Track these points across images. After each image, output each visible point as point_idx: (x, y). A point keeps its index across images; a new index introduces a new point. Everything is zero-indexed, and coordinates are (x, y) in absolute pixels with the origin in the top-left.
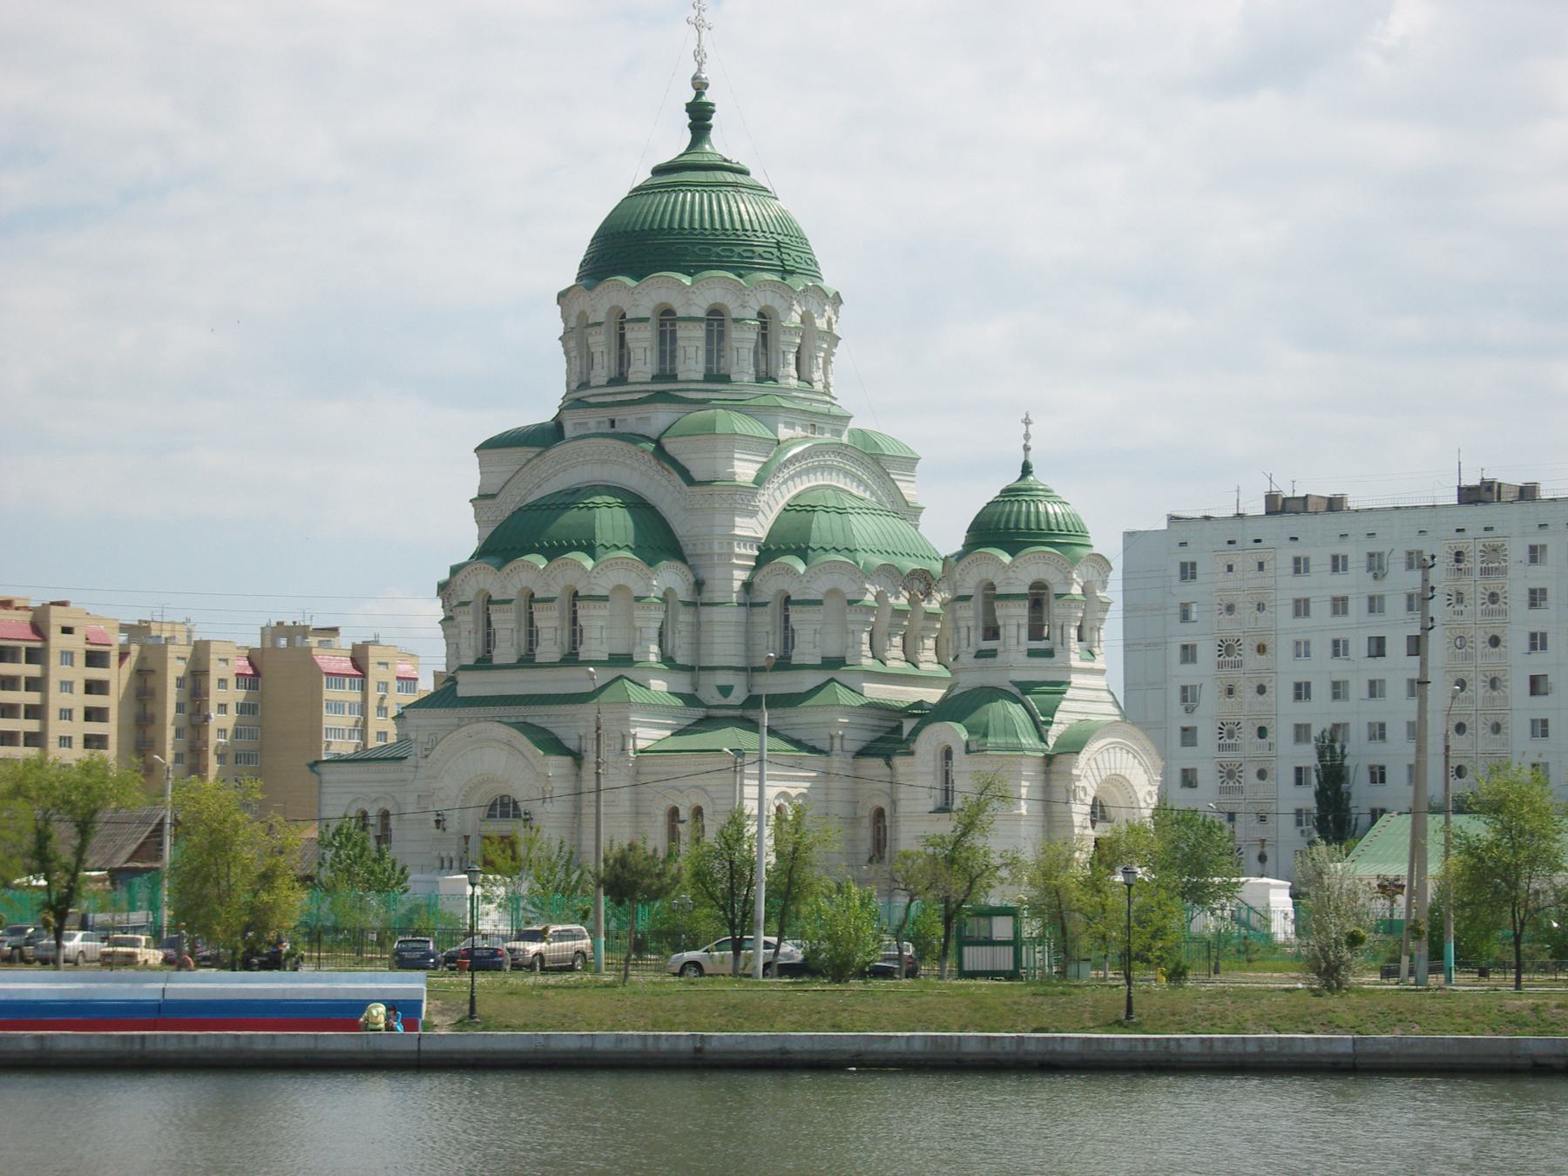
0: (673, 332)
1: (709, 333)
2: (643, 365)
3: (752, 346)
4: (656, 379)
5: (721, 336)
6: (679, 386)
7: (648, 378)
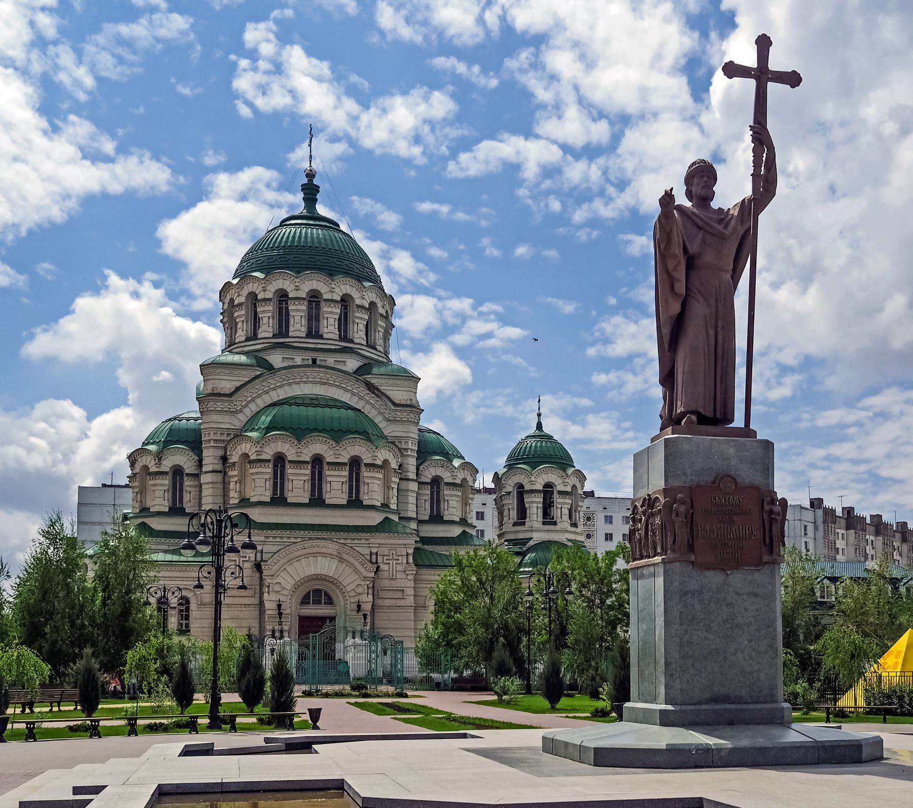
0: (287, 308)
1: (310, 308)
2: (267, 329)
3: (337, 317)
4: (274, 336)
5: (318, 308)
6: (290, 340)
7: (271, 335)
